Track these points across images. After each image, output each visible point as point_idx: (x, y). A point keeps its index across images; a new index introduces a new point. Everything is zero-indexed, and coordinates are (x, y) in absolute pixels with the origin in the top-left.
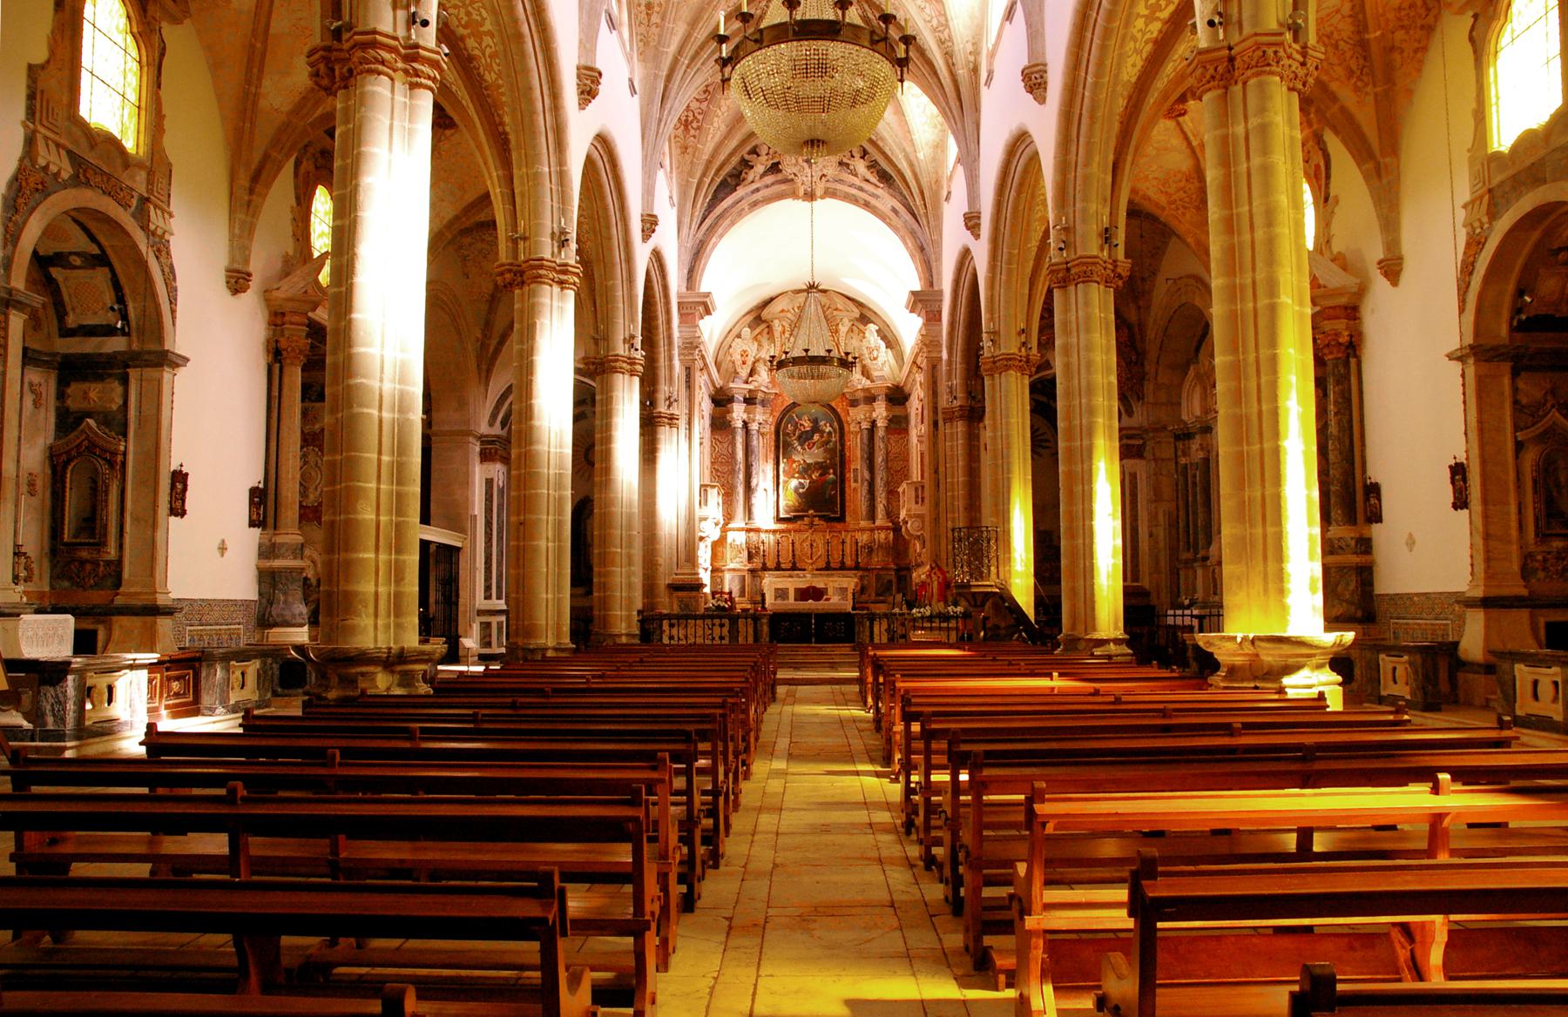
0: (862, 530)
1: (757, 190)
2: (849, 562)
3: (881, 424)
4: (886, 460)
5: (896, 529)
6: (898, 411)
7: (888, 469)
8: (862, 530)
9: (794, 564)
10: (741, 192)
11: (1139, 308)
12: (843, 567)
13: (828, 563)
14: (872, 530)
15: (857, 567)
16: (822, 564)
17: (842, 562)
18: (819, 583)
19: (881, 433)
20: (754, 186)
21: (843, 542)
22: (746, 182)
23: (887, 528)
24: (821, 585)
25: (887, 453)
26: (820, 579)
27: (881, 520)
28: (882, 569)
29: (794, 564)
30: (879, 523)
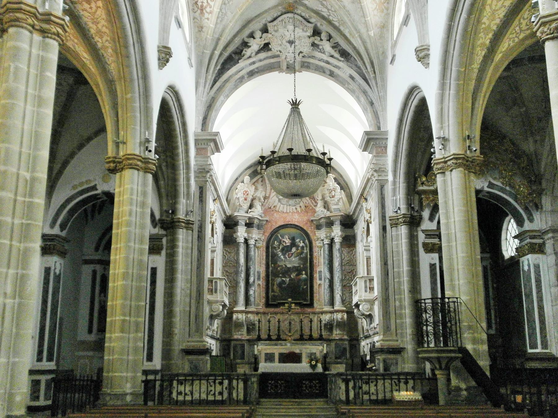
0: (326, 312)
1: (254, 63)
2: (315, 335)
3: (338, 240)
4: (341, 265)
5: (350, 313)
6: (349, 232)
7: (342, 271)
8: (326, 312)
9: (279, 336)
10: (242, 64)
11: (536, 141)
12: (311, 338)
13: (302, 336)
14: (331, 312)
15: (321, 338)
16: (297, 336)
17: (311, 336)
18: (296, 349)
19: (337, 246)
20: (251, 60)
21: (311, 321)
22: (246, 57)
23: (342, 311)
24: (297, 351)
25: (342, 260)
26: (297, 347)
27: (338, 306)
28: (341, 340)
29: (279, 336)
30: (336, 308)
